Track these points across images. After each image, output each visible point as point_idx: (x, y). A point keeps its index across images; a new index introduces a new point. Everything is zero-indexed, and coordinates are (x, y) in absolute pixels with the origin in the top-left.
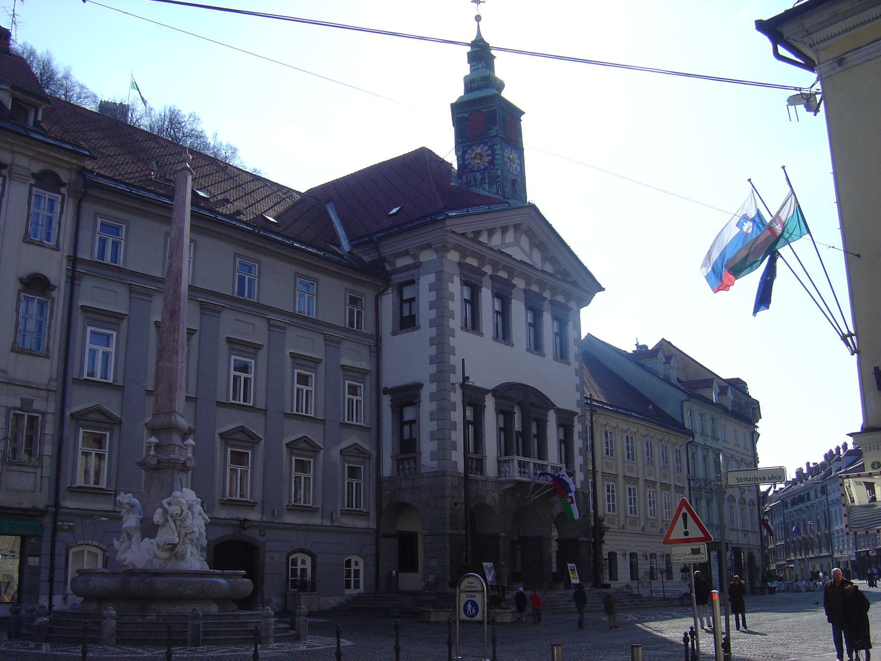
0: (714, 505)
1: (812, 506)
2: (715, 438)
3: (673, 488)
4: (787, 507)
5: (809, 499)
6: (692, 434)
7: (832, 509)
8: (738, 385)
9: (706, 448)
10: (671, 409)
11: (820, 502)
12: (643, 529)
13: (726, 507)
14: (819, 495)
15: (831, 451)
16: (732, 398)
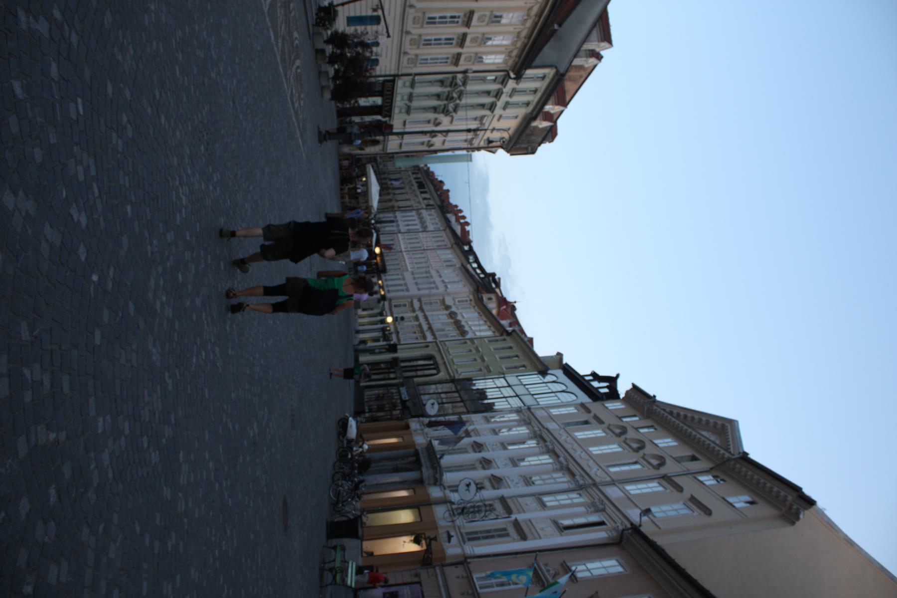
0: (434, 103)
1: (417, 196)
2: (506, 106)
3: (459, 50)
4: (413, 173)
5: (422, 193)
6: (519, 77)
7: (414, 213)
8: (551, 134)
9: (498, 94)
10: (548, 52)
11: (419, 202)
12: (412, 6)
13: (431, 116)
14: (426, 202)
15: (461, 211)
16: (541, 126)
